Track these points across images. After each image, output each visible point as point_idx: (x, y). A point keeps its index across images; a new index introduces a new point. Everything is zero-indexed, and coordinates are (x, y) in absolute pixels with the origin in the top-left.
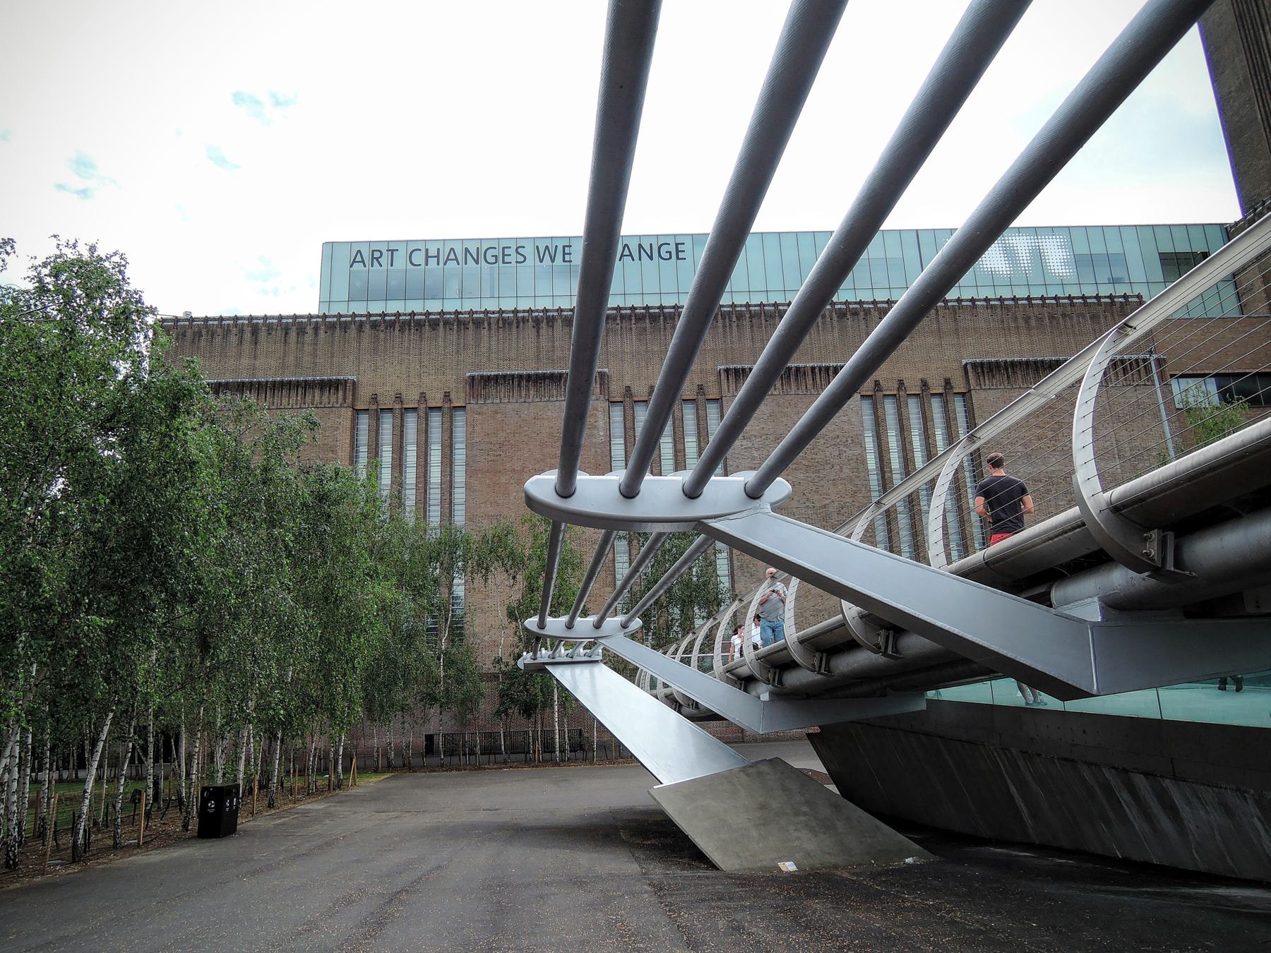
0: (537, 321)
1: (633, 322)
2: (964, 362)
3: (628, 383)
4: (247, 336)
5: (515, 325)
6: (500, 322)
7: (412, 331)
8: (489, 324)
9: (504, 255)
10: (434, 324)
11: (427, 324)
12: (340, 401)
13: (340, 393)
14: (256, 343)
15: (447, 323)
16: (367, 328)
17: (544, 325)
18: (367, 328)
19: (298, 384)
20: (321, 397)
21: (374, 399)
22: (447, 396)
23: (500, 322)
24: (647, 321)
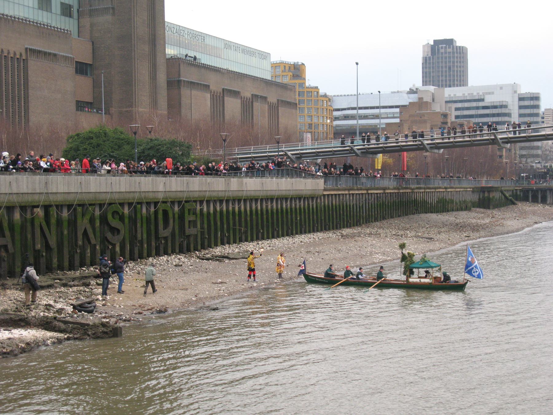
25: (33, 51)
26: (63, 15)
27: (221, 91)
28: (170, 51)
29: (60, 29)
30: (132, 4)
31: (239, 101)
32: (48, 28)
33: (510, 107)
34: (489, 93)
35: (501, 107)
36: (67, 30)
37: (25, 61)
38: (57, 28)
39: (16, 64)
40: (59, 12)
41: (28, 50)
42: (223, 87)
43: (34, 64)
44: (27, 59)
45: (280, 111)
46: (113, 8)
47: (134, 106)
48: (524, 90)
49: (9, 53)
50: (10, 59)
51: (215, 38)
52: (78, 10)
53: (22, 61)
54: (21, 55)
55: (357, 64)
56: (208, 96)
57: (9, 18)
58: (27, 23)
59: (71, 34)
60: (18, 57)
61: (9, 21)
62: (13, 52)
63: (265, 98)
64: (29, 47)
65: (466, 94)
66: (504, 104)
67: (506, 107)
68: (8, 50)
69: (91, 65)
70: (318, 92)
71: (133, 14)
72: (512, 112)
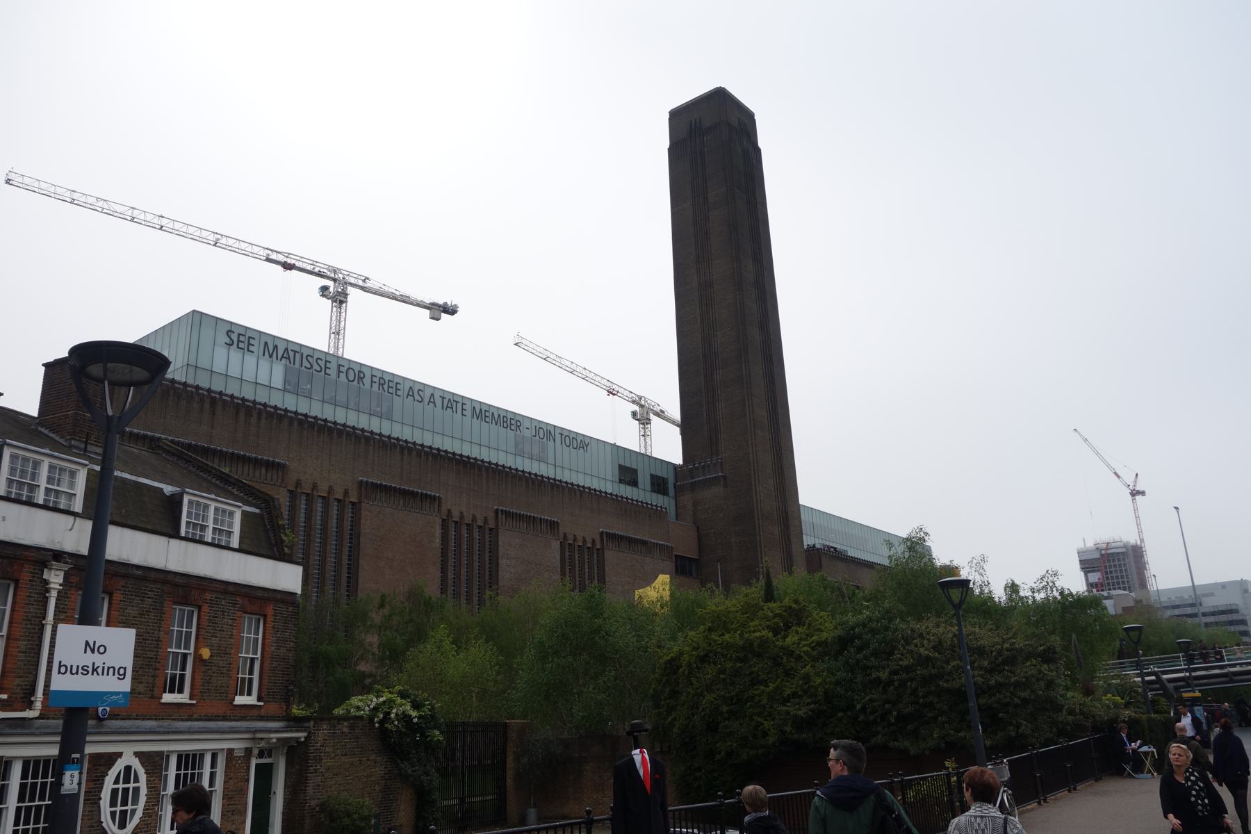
0: (402, 448)
1: (454, 463)
2: (601, 530)
3: (449, 507)
4: (207, 406)
5: (389, 448)
6: (381, 443)
7: (326, 434)
8: (374, 443)
9: (326, 368)
10: (340, 433)
11: (335, 431)
12: (280, 481)
13: (280, 474)
14: (214, 414)
15: (348, 434)
16: (296, 424)
17: (406, 452)
18: (296, 424)
19: (250, 460)
20: (266, 474)
21: (298, 483)
22: (346, 493)
23: (381, 443)
24: (462, 465)
25: (611, 537)
26: (654, 492)
28: (808, 541)
29: (651, 505)
30: (752, 468)
32: (632, 503)
34: (1207, 595)
35: (1231, 611)
36: (661, 507)
37: (601, 552)
38: (647, 503)
39: (586, 557)
40: (648, 487)
41: (604, 534)
43: (613, 557)
44: (603, 548)
46: (724, 477)
49: (575, 540)
50: (576, 548)
52: (674, 484)
53: (595, 551)
54: (594, 542)
55: (1177, 508)
57: (575, 487)
58: (601, 496)
59: (666, 512)
60: (589, 545)
61: (575, 492)
62: (582, 539)
64: (605, 530)
65: (1173, 598)
66: (1234, 607)
67: (1236, 611)
68: (575, 536)
71: (753, 483)
72: (1247, 618)
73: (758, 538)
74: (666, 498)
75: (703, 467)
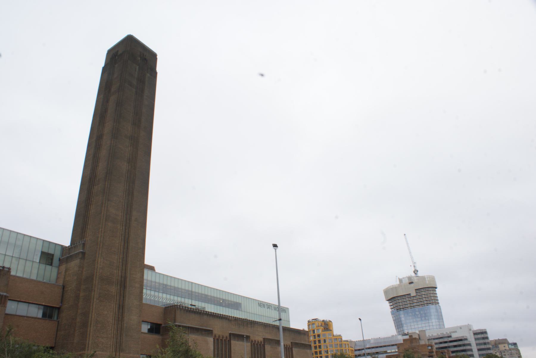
27: (228, 335)
31: (249, 344)
33: (469, 339)
34: (454, 332)
42: (230, 332)
45: (294, 352)
46: (83, 254)
47: (87, 349)
48: (476, 327)
51: (250, 299)
56: (211, 340)
63: (248, 337)
65: (439, 334)
66: (465, 338)
67: (466, 339)
69: (59, 309)
70: (341, 339)
71: (97, 256)
72: (471, 343)
73: (93, 293)
74: (49, 267)
75: (75, 247)
